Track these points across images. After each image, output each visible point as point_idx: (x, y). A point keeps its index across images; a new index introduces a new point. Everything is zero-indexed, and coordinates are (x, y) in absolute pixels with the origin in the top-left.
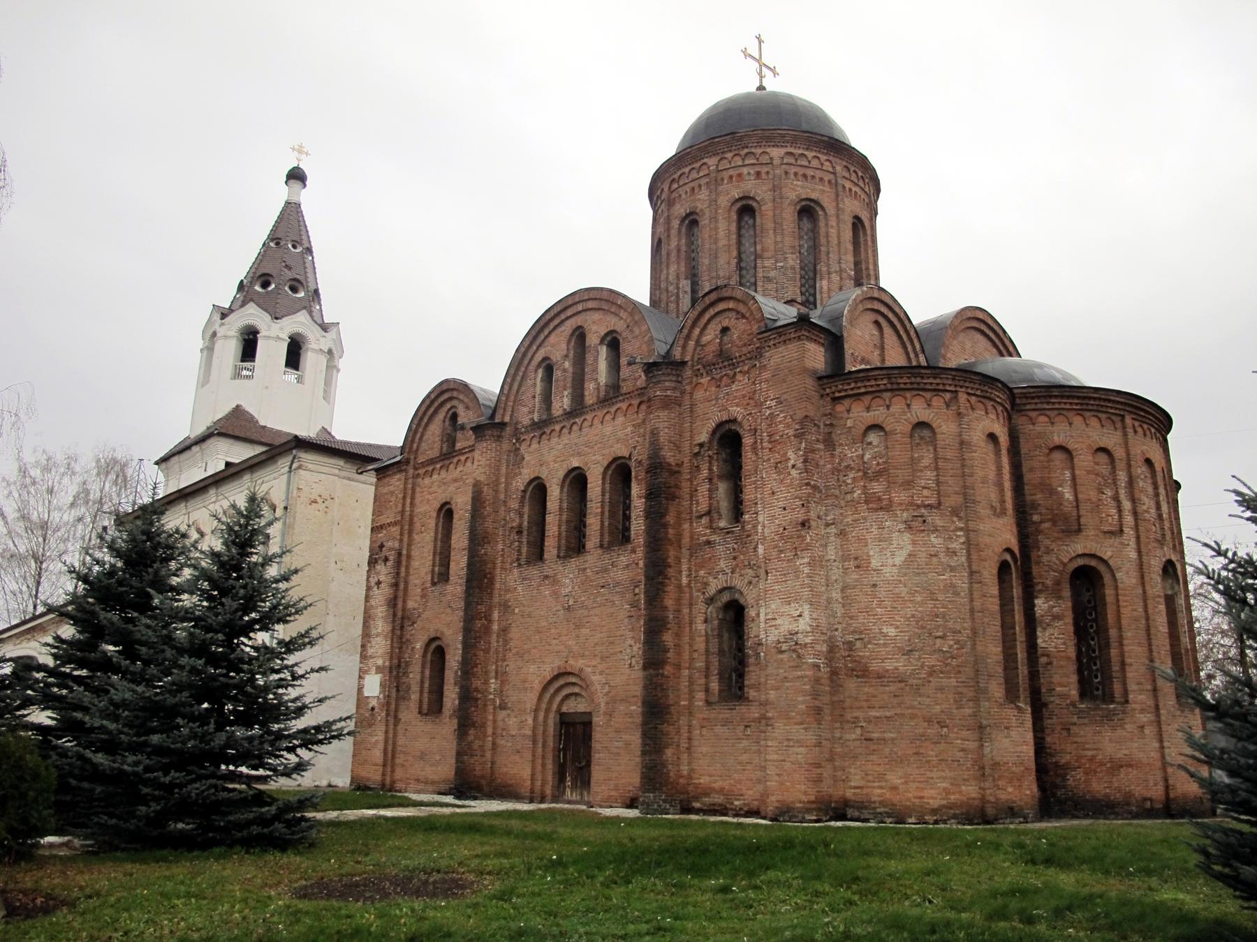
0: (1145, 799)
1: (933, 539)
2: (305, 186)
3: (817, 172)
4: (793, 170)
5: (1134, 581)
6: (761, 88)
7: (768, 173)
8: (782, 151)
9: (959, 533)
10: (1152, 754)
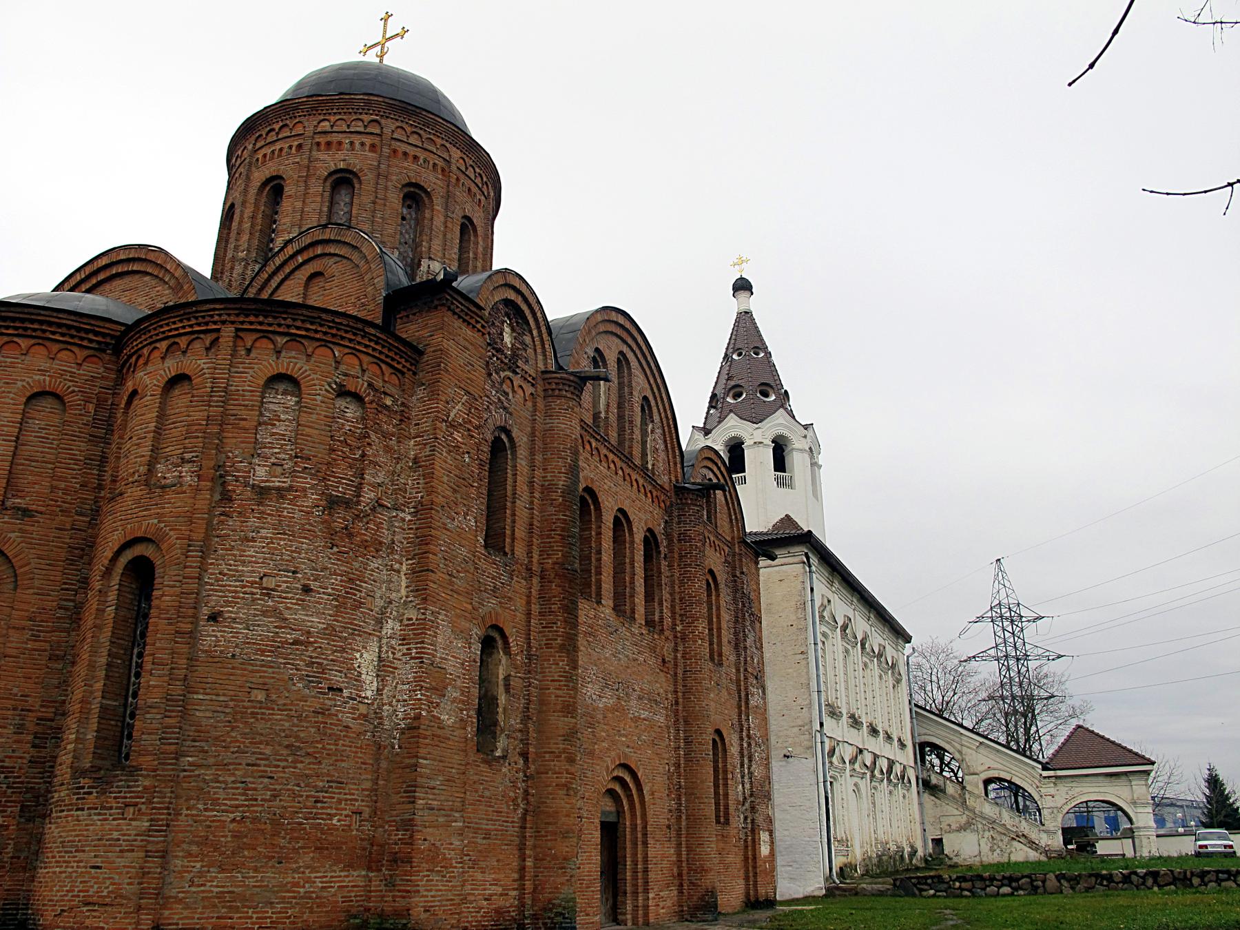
2: (752, 294)
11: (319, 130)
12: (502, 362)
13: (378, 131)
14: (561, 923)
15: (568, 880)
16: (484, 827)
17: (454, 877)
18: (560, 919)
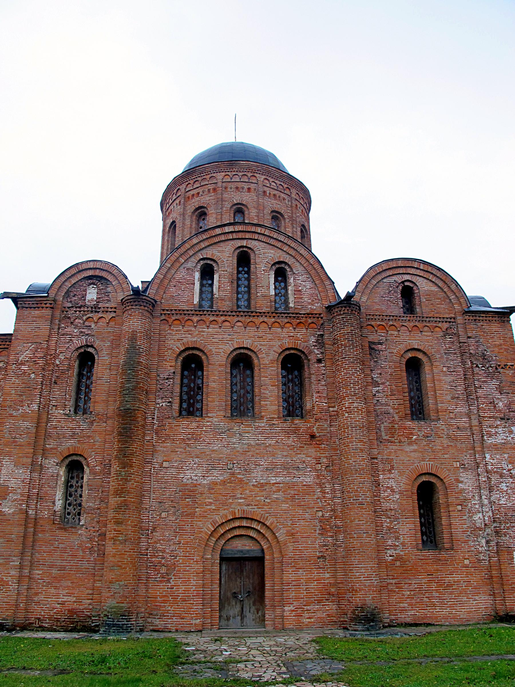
12: (84, 311)
14: (106, 621)
15: (112, 595)
16: (58, 564)
17: (11, 591)
18: (105, 618)
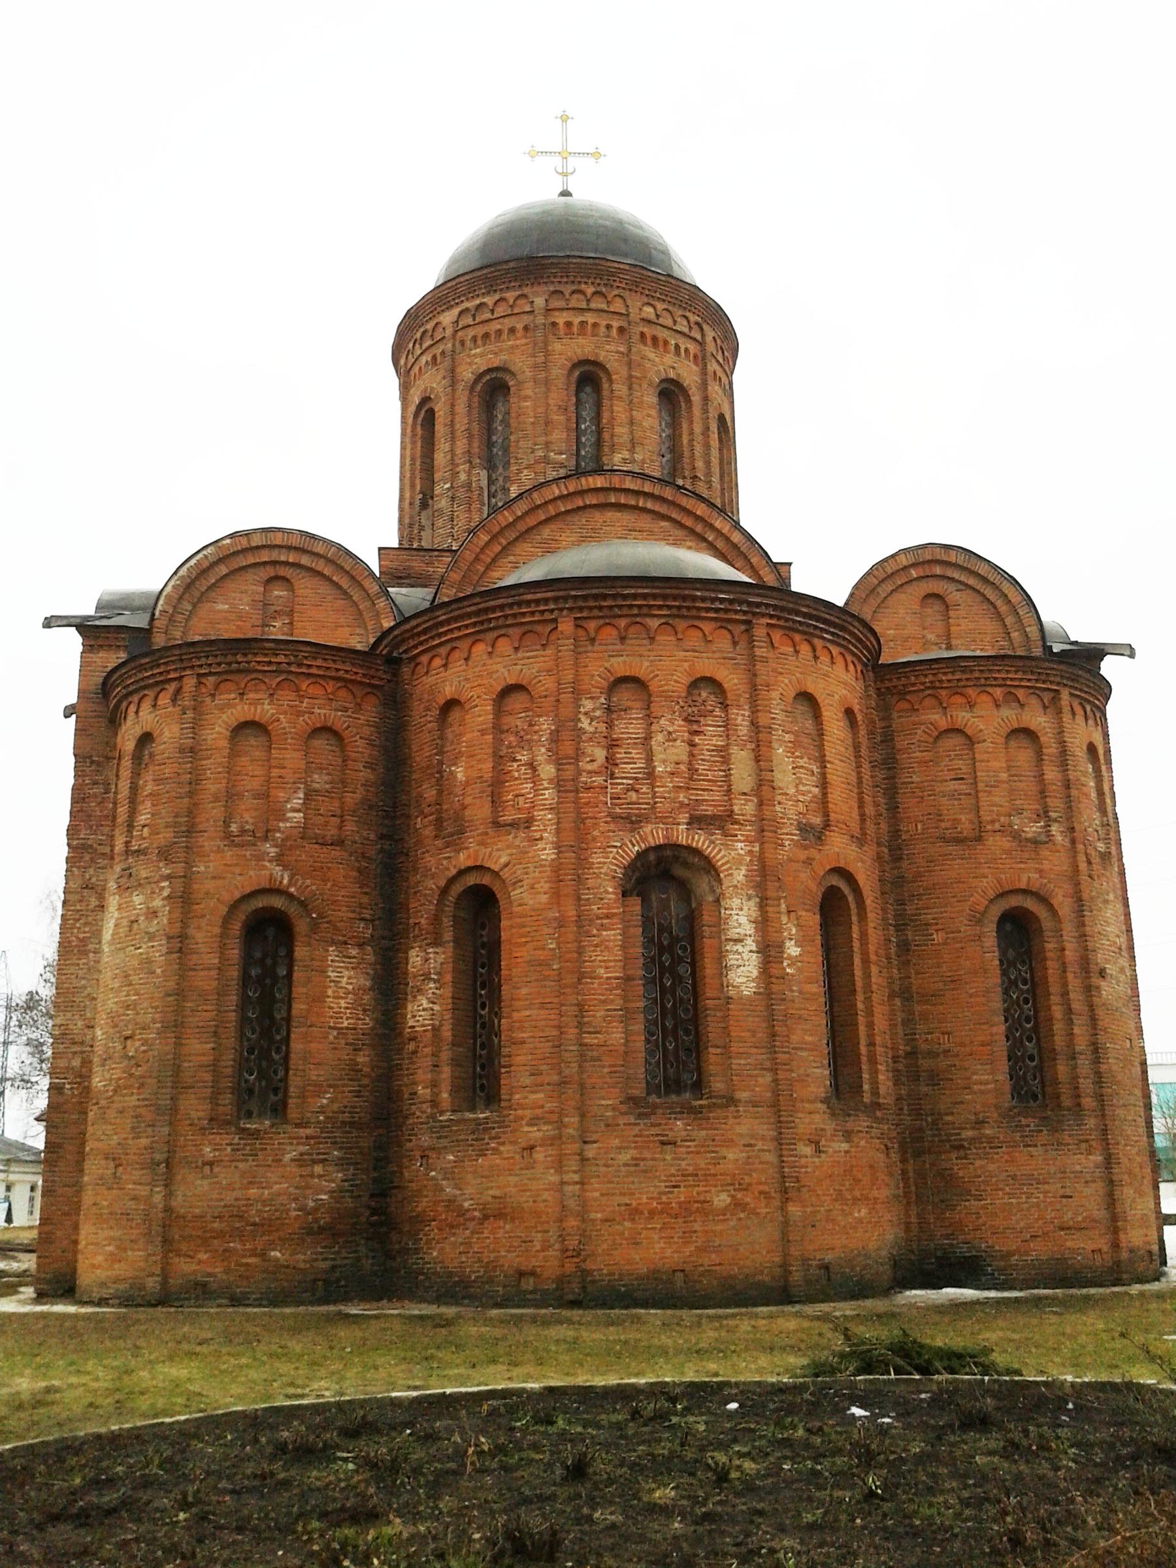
0: (521, 1274)
1: (137, 899)
3: (506, 320)
4: (471, 333)
5: (544, 898)
6: (565, 193)
7: (443, 353)
8: (456, 311)
9: (163, 884)
10: (545, 1195)
11: (644, 315)
13: (699, 337)
